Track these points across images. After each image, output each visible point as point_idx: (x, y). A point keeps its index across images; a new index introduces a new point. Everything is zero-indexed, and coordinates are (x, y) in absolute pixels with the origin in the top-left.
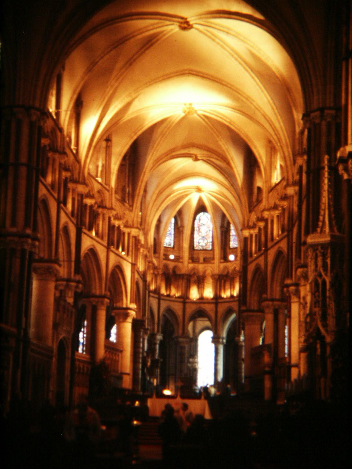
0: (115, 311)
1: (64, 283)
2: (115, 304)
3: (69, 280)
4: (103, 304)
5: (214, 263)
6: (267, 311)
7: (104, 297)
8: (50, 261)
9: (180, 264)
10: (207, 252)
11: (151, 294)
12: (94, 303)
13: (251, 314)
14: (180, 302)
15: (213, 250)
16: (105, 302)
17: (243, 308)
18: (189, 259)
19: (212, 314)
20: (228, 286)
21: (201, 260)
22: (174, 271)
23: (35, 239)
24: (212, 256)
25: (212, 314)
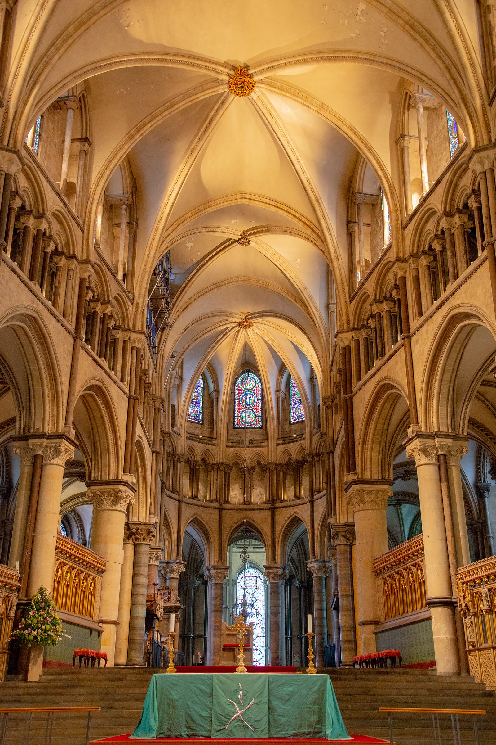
2: (92, 475)
4: (57, 452)
5: (267, 446)
6: (420, 459)
7: (61, 436)
9: (214, 447)
10: (254, 430)
11: (166, 490)
12: (40, 453)
14: (214, 508)
15: (265, 426)
16: (63, 449)
17: (352, 477)
18: (228, 440)
19: (266, 529)
20: (289, 482)
21: (247, 443)
22: (204, 460)
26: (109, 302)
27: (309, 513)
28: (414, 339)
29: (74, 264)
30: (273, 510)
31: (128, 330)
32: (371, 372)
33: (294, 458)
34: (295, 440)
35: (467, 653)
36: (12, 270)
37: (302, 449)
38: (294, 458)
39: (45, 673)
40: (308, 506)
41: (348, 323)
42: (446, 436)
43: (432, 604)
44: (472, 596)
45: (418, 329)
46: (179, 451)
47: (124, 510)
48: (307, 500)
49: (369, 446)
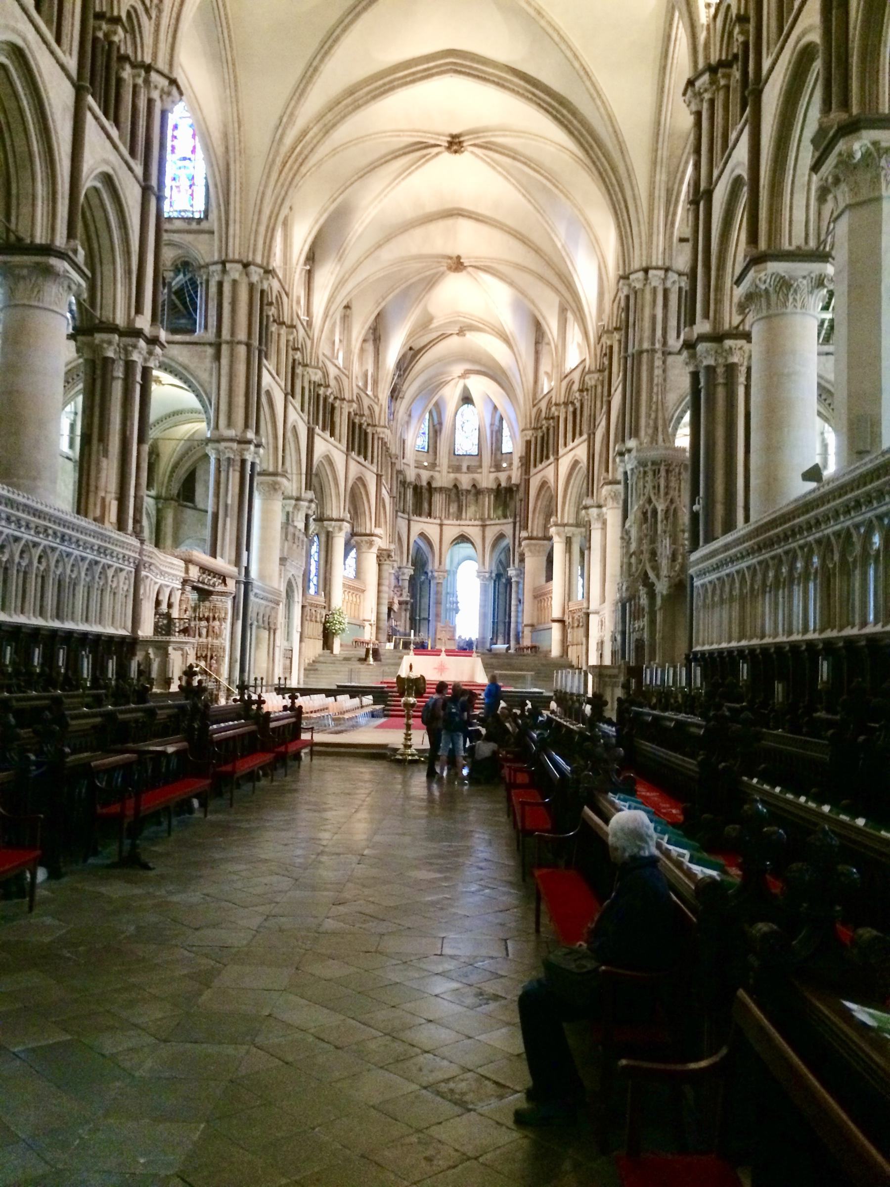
0: (356, 538)
1: (293, 502)
3: (298, 499)
5: (481, 473)
6: (556, 539)
7: (343, 520)
8: (275, 474)
9: (437, 474)
11: (400, 514)
12: (331, 529)
13: (533, 542)
15: (480, 454)
17: (524, 534)
18: (449, 467)
19: (478, 541)
21: (464, 469)
22: (429, 484)
23: (258, 446)
24: (478, 464)
25: (478, 541)
26: (364, 415)
27: (512, 531)
28: (560, 461)
29: (345, 405)
30: (484, 526)
31: (375, 426)
32: (540, 467)
33: (503, 484)
34: (504, 470)
35: (568, 646)
36: (319, 435)
37: (509, 478)
38: (503, 484)
39: (342, 650)
40: (511, 526)
41: (531, 423)
42: (572, 525)
43: (554, 621)
44: (573, 618)
45: (563, 456)
46: (408, 480)
47: (376, 551)
48: (511, 520)
49: (537, 515)
